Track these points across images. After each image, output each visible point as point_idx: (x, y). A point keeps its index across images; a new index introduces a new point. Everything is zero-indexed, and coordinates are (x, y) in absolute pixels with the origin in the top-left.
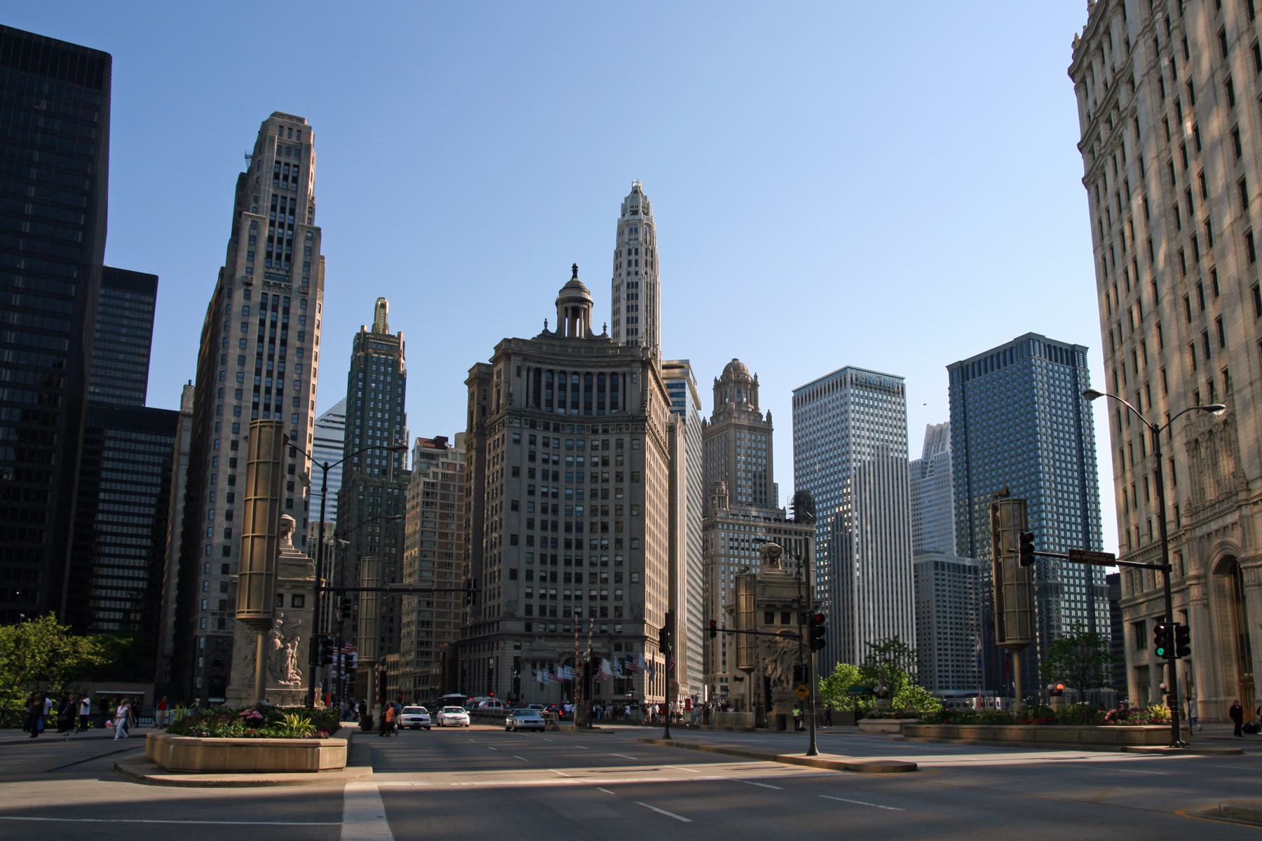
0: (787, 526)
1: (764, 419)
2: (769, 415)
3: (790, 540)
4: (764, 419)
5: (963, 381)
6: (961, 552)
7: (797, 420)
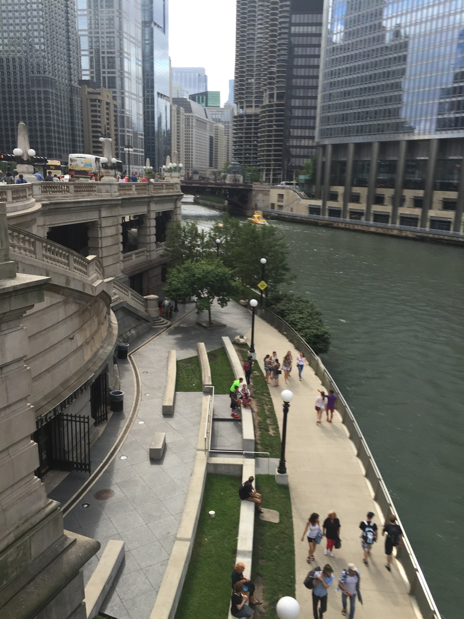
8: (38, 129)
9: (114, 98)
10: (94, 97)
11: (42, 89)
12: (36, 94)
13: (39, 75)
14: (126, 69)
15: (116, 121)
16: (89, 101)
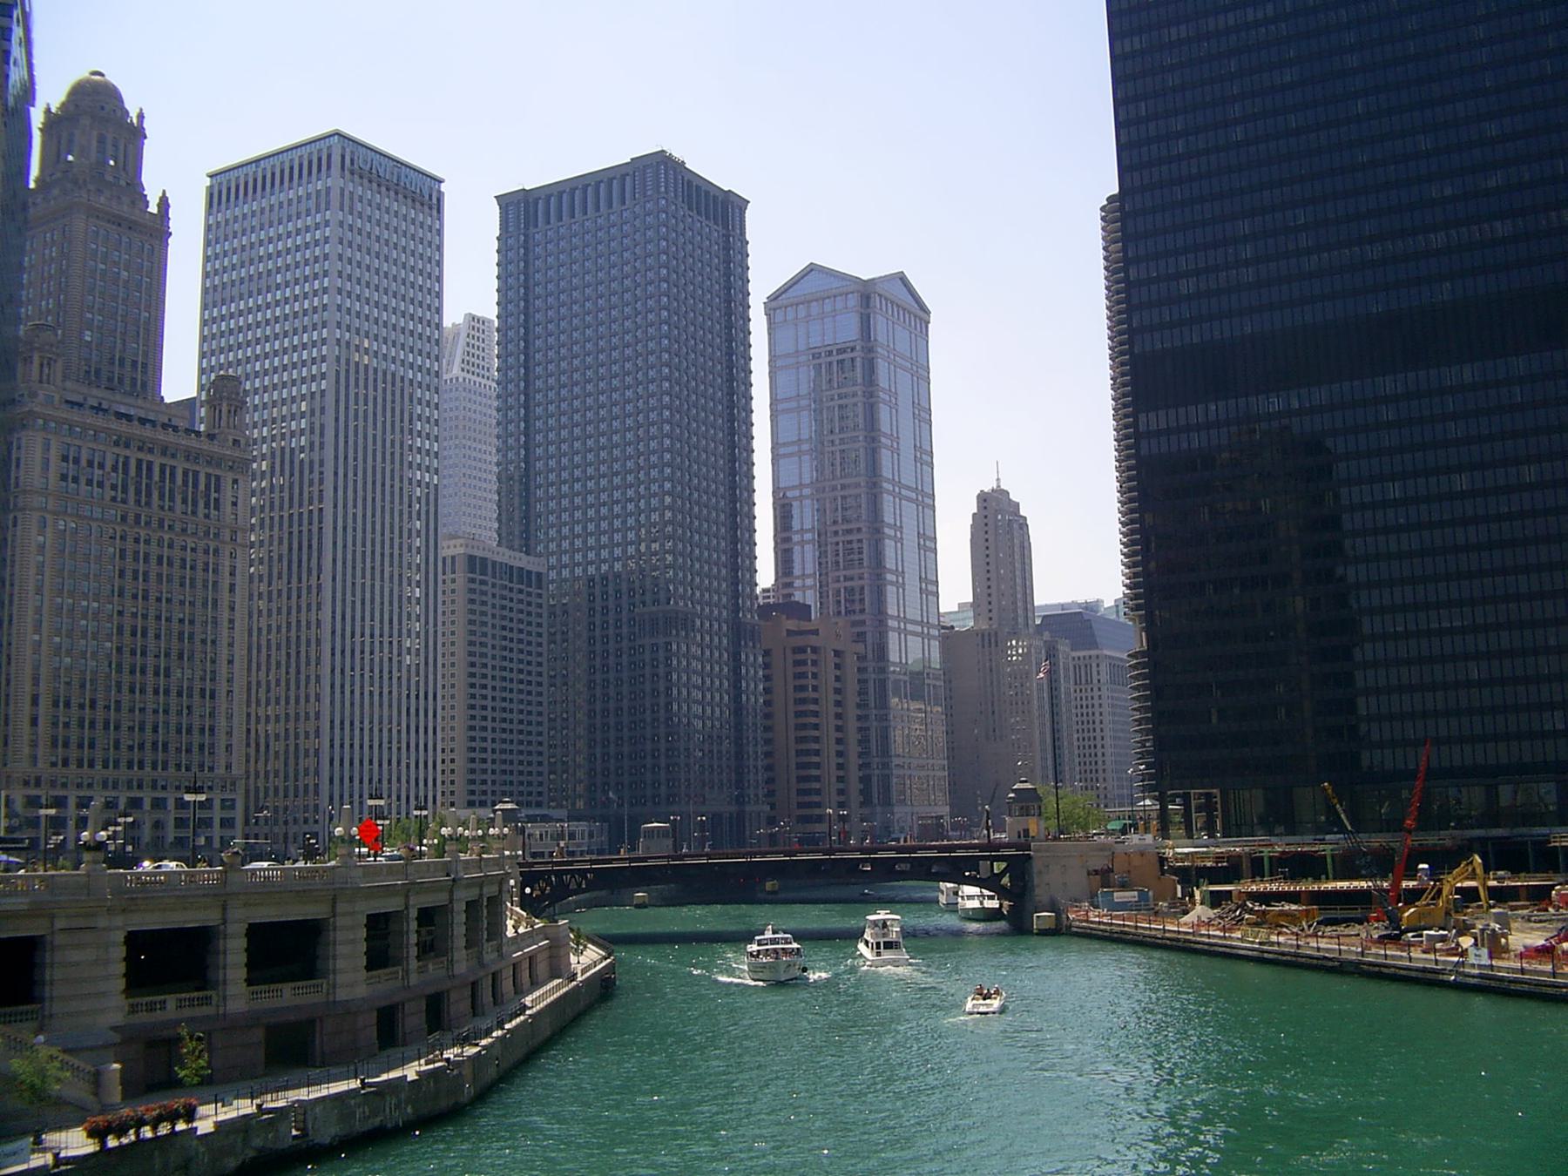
0: (192, 442)
1: (153, 209)
2: (164, 203)
3: (196, 474)
4: (153, 209)
5: (527, 227)
6: (504, 539)
7: (214, 236)
8: (648, 736)
9: (860, 637)
10: (798, 641)
11: (661, 640)
12: (647, 652)
13: (654, 609)
14: (890, 563)
15: (862, 692)
16: (789, 652)
